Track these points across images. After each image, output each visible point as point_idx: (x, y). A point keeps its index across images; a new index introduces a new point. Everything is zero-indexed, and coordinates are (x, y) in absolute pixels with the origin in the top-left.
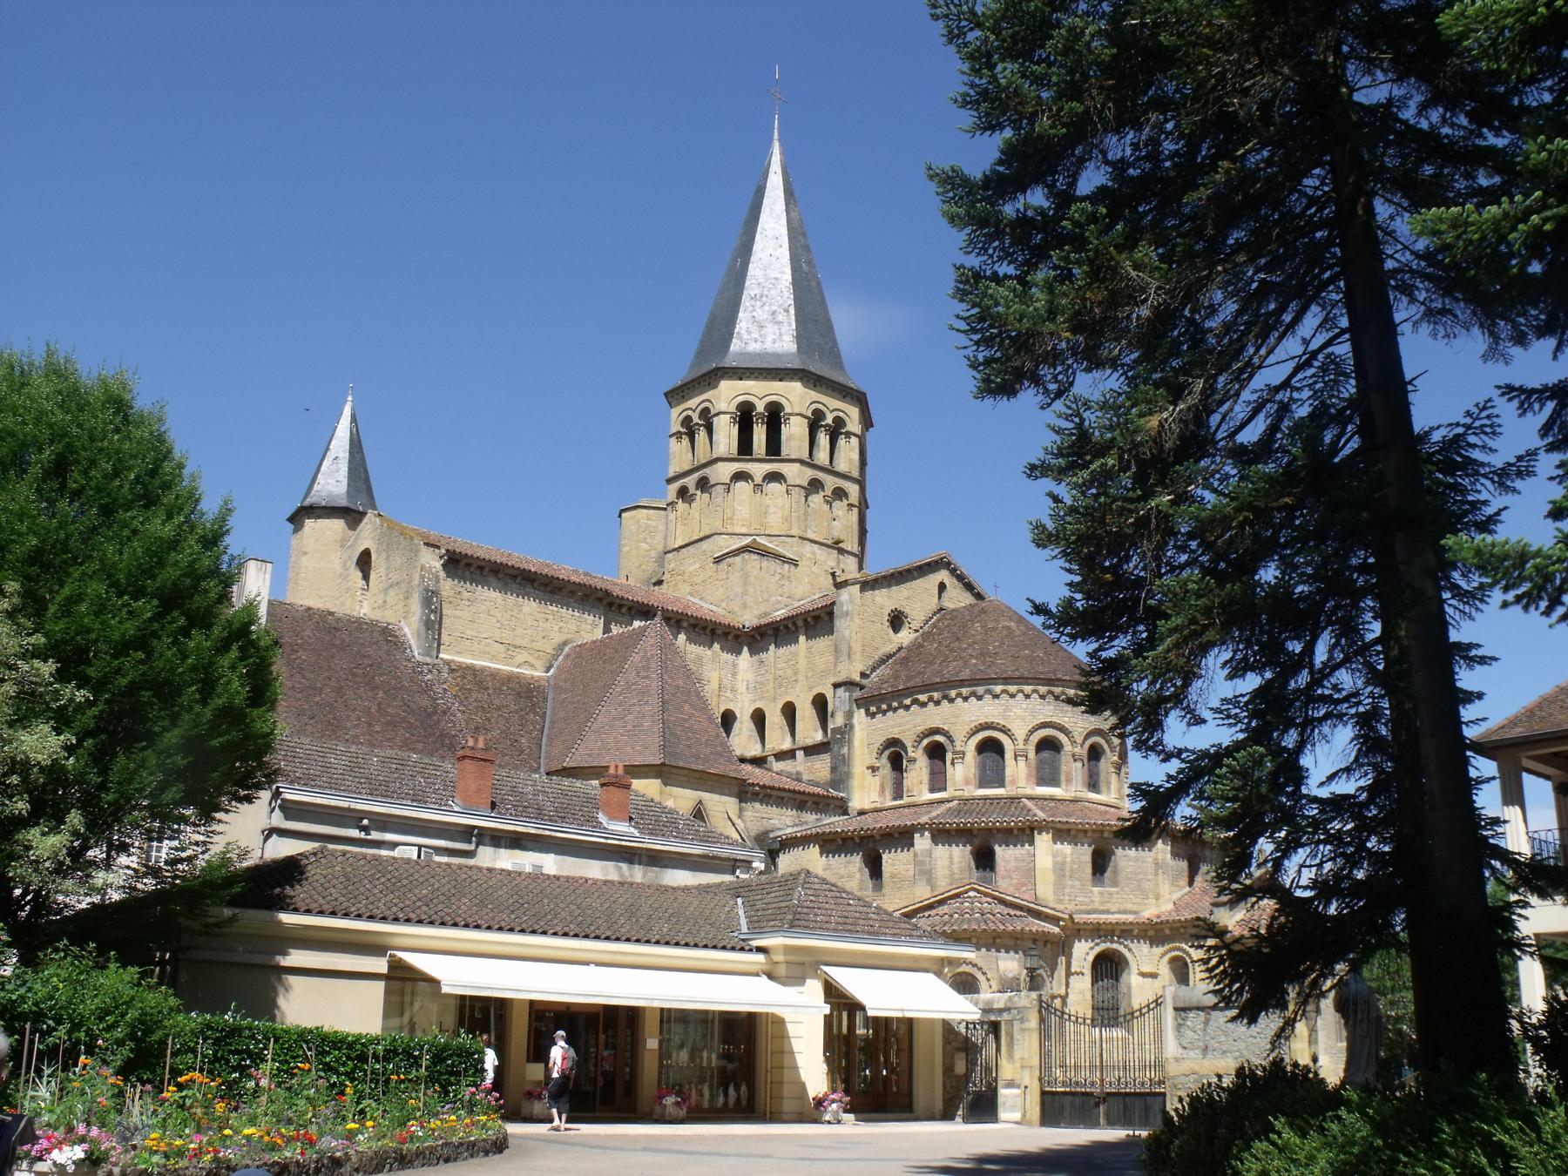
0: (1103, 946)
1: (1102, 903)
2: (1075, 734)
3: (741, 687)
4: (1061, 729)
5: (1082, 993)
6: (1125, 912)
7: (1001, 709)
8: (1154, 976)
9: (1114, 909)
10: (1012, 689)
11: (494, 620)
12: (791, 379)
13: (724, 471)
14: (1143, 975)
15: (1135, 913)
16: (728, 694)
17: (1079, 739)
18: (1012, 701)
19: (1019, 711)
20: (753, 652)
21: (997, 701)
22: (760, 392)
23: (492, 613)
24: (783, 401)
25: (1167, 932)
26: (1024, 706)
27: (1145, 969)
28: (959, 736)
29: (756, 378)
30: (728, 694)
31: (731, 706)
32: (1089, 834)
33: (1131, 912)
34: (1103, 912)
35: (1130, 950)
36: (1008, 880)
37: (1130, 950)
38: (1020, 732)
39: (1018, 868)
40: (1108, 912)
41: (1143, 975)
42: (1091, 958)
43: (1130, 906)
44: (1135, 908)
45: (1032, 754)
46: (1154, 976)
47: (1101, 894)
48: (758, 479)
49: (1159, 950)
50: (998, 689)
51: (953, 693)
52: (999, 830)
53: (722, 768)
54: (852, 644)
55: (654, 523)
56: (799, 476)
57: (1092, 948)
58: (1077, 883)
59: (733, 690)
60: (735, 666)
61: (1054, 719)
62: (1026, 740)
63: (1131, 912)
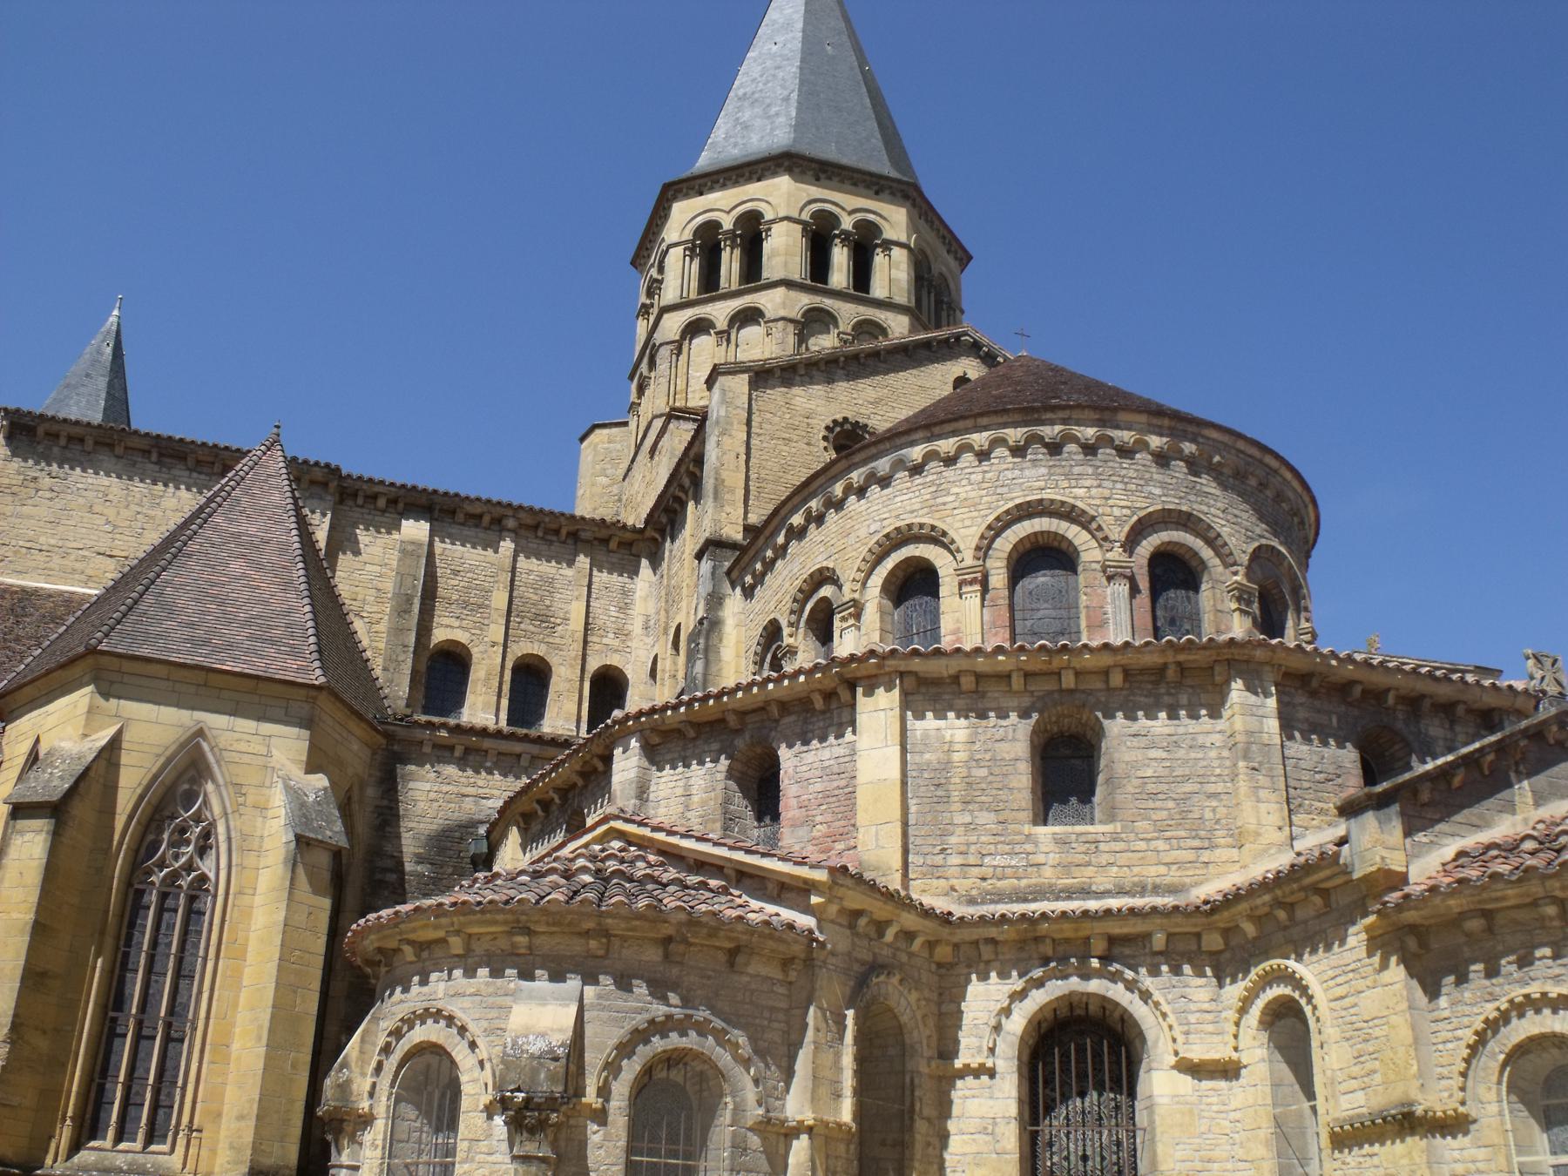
0: (1056, 989)
1: (1066, 867)
2: (1106, 522)
3: (636, 627)
4: (1070, 514)
5: (988, 1129)
6: (1142, 890)
7: (926, 493)
8: (1228, 1071)
9: (1102, 882)
10: (947, 445)
11: (100, 521)
12: (775, 174)
13: (673, 325)
14: (1196, 1070)
15: (1173, 890)
16: (609, 639)
17: (1119, 533)
18: (950, 473)
19: (963, 490)
20: (656, 562)
21: (918, 480)
22: (723, 205)
23: (97, 508)
24: (762, 207)
25: (1250, 929)
26: (977, 477)
27: (1197, 1053)
28: (848, 573)
29: (724, 186)
30: (609, 639)
31: (614, 660)
32: (1017, 682)
33: (1156, 889)
34: (1070, 893)
35: (1146, 996)
36: (802, 832)
37: (1146, 996)
38: (967, 534)
39: (826, 795)
40: (1085, 892)
41: (1196, 1070)
42: (1017, 1023)
43: (1152, 873)
44: (1173, 876)
45: (998, 579)
46: (1228, 1071)
47: (1061, 842)
48: (721, 324)
49: (1234, 991)
50: (916, 453)
51: (838, 489)
52: (784, 706)
53: (261, 663)
54: (724, 474)
55: (619, 446)
56: (784, 305)
57: (1020, 995)
58: (986, 818)
59: (622, 633)
60: (625, 593)
61: (1048, 495)
62: (983, 550)
63: (1156, 889)
